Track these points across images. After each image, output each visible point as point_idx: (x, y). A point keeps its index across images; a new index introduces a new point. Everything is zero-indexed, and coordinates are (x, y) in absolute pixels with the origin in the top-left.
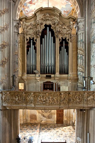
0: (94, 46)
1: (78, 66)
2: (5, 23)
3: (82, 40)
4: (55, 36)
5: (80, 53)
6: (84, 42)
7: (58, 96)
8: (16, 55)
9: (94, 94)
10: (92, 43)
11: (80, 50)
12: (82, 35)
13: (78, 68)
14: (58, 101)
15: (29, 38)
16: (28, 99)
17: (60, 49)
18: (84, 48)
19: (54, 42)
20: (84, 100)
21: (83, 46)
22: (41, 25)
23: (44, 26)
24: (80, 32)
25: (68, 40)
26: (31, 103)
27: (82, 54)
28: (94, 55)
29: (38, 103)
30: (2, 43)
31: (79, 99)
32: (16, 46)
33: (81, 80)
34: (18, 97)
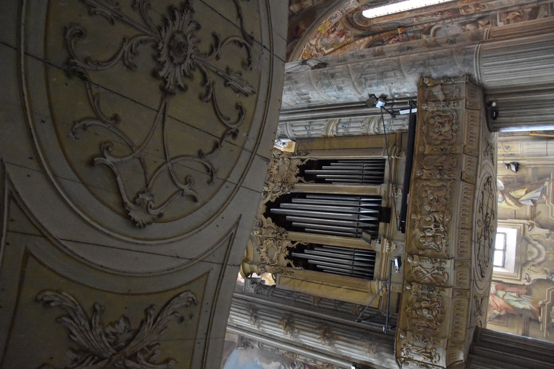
0: (314, 98)
1: (365, 132)
2: (244, 310)
3: (305, 126)
4: (291, 193)
5: (335, 129)
6: (311, 122)
7: (427, 186)
8: (322, 302)
9: (429, 85)
10: (310, 102)
11: (327, 129)
12: (296, 126)
13: (373, 132)
14: (440, 187)
15: (285, 258)
16: (431, 278)
17: (322, 181)
18: (323, 121)
19: (303, 195)
20: (444, 111)
21: (318, 123)
22: (264, 226)
23: (267, 218)
24: (289, 130)
25: (302, 160)
26: (440, 268)
27: (337, 125)
28: (334, 96)
29: (444, 246)
30: (280, 326)
31: (442, 124)
32: (299, 298)
33: (401, 123)
34: (421, 308)
